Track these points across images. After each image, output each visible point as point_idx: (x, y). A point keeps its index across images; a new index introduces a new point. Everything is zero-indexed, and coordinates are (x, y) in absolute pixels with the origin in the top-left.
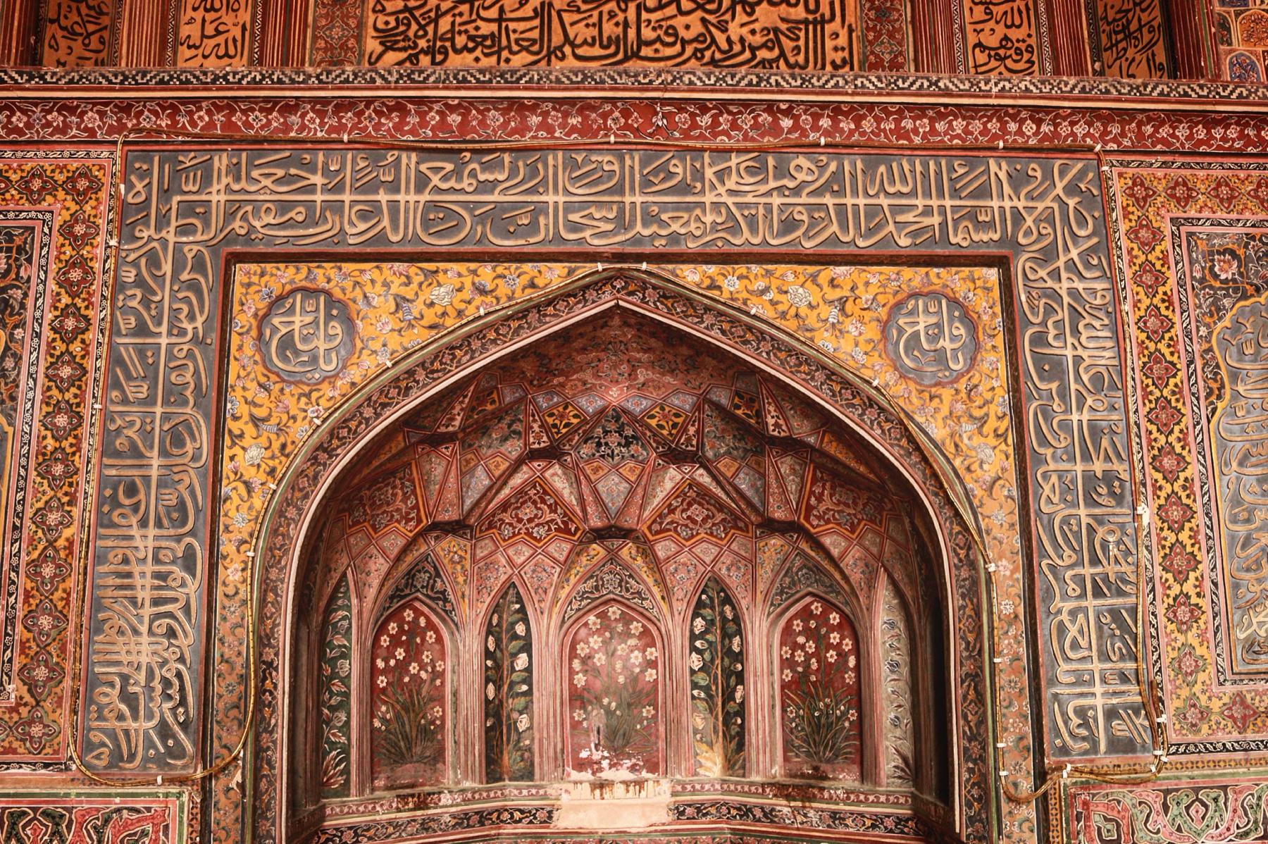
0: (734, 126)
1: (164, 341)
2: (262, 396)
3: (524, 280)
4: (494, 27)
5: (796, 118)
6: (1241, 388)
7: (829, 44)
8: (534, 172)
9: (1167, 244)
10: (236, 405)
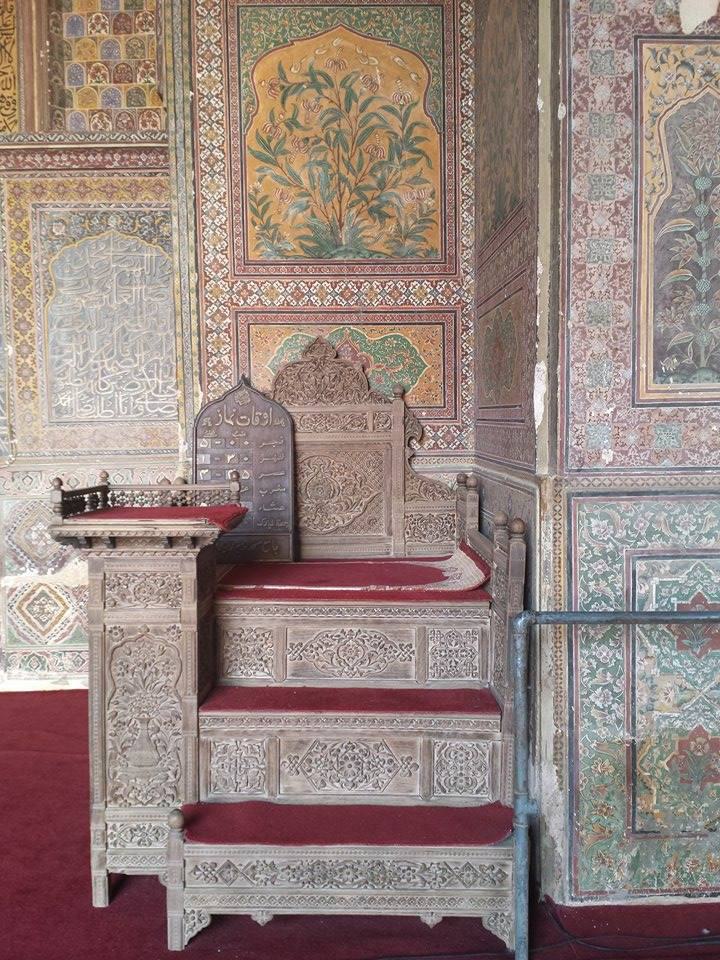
6: (61, 290)
9: (29, 218)
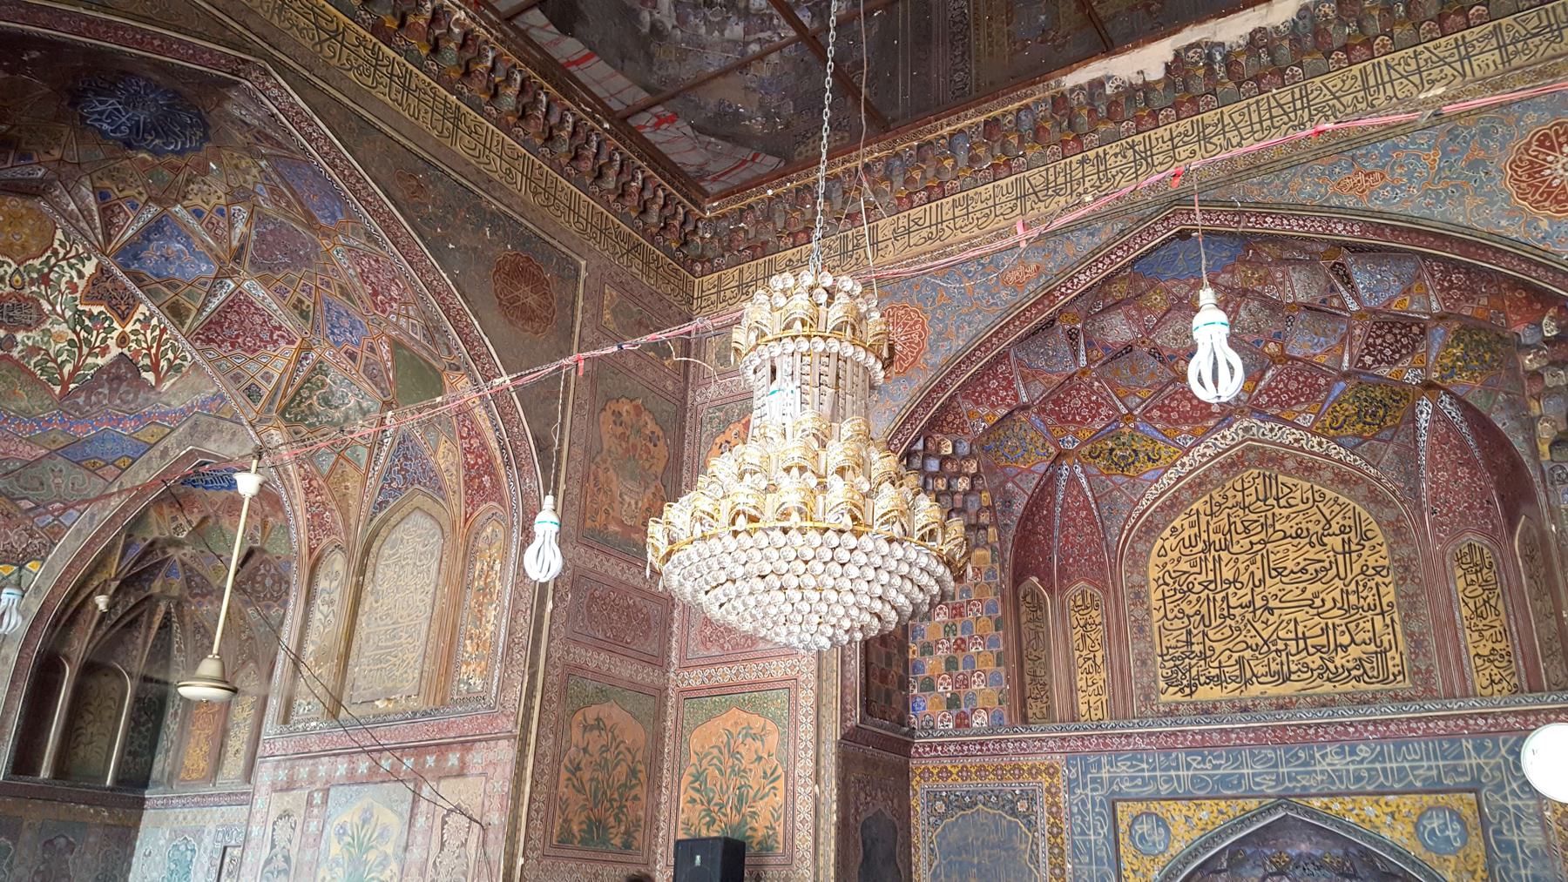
0: (1326, 733)
1: (1092, 838)
2: (1135, 861)
3: (1239, 808)
4: (1217, 671)
5: (1356, 727)
7: (1390, 663)
8: (1236, 759)
10: (1125, 864)
